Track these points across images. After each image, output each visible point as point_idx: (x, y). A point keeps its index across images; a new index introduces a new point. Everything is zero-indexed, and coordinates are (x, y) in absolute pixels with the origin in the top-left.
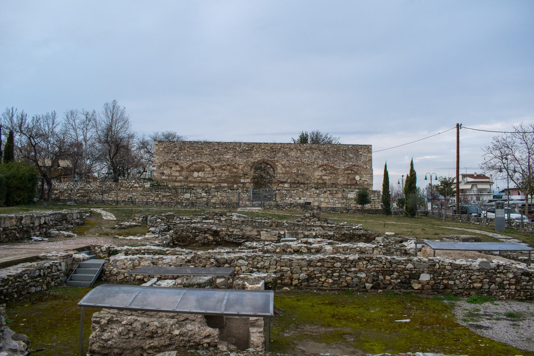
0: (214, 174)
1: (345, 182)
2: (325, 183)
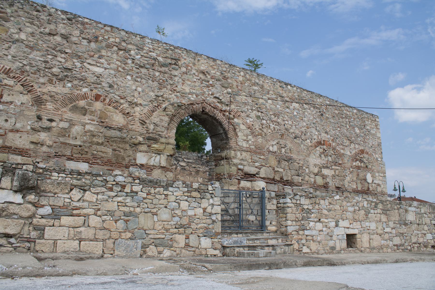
0: (39, 118)
2: (326, 186)
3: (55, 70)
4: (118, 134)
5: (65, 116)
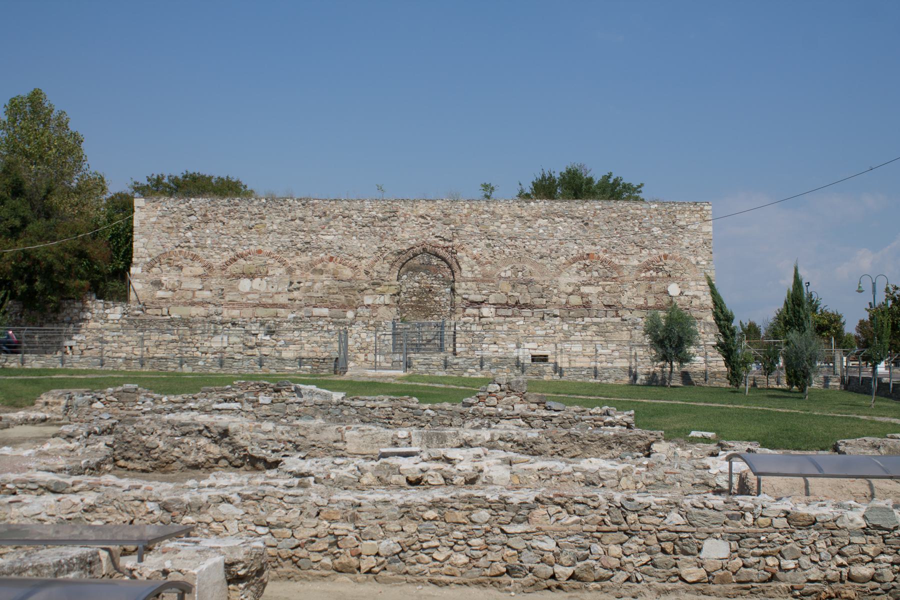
1: (641, 302)
2: (587, 306)
3: (299, 245)
4: (348, 284)
5: (309, 278)
